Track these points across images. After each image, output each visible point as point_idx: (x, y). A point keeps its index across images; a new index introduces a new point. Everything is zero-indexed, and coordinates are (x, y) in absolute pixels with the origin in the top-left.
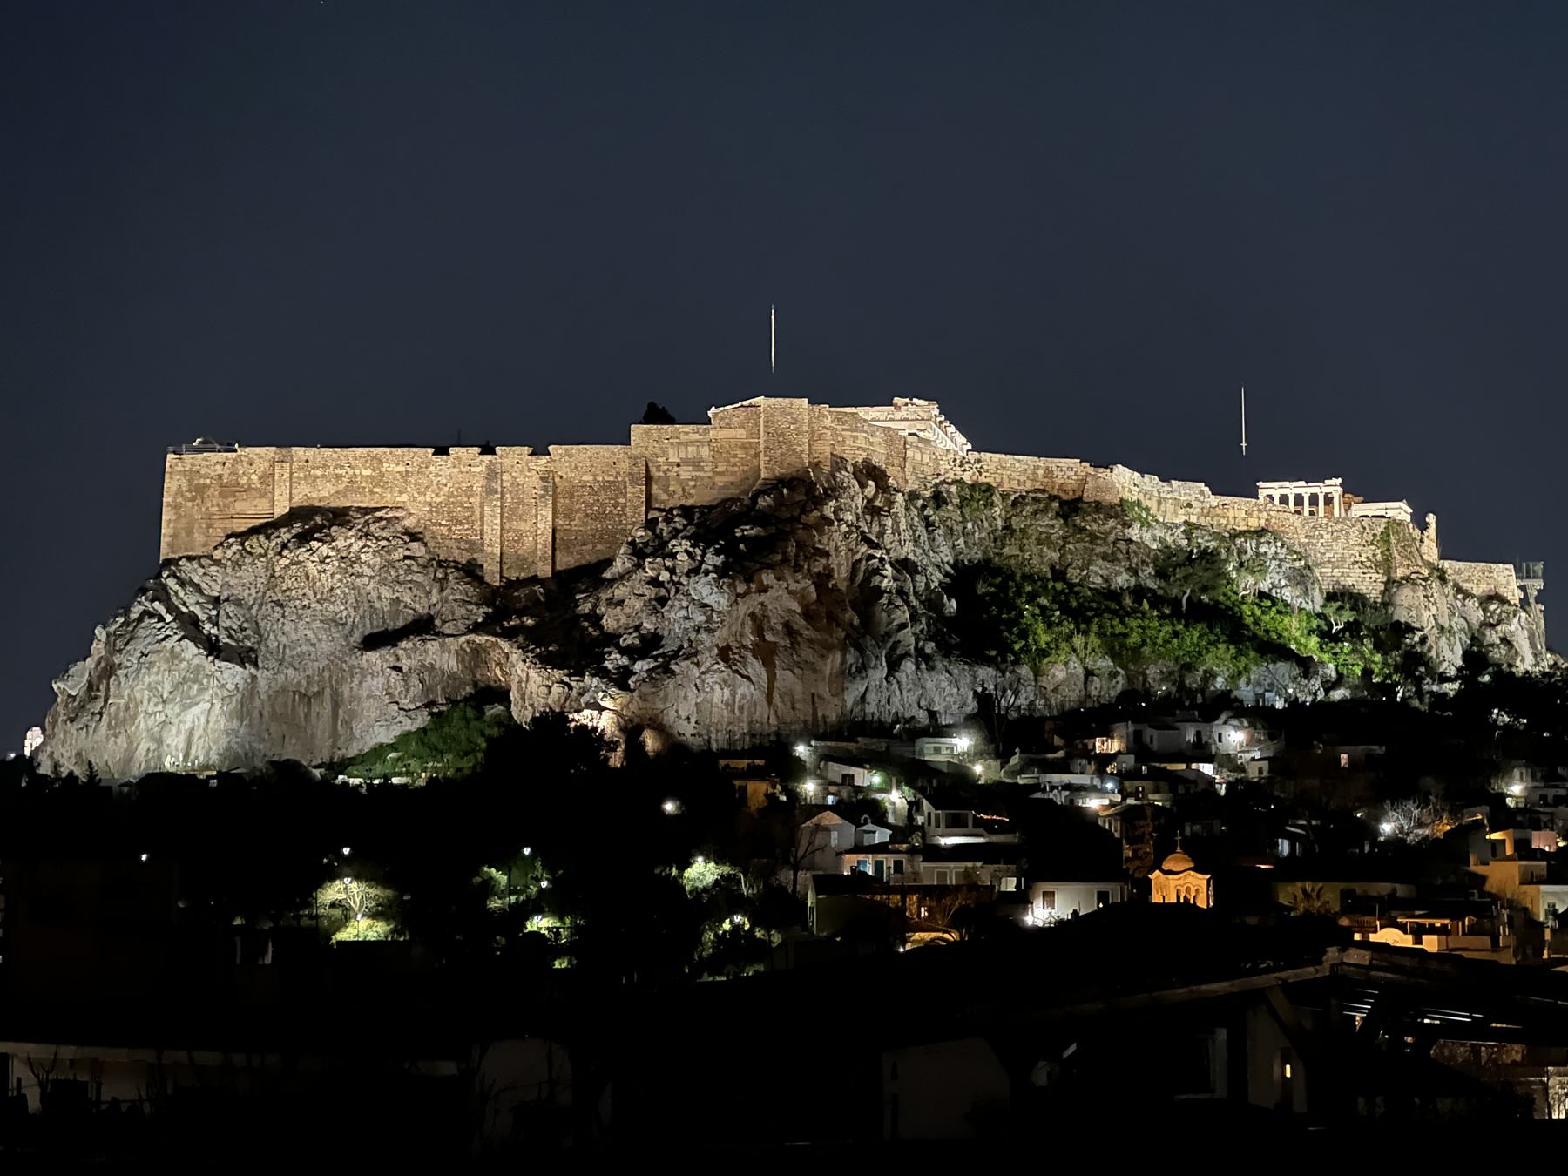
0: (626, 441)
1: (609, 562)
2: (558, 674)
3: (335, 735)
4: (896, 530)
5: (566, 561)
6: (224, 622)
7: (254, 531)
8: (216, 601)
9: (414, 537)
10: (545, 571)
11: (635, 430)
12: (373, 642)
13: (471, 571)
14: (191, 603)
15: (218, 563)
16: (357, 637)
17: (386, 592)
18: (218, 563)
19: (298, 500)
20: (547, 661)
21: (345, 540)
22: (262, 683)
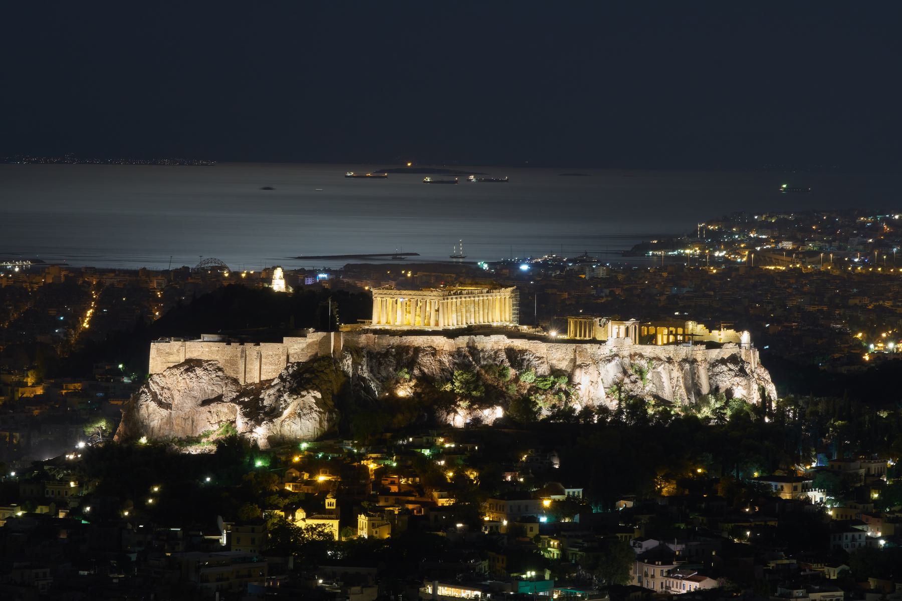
0: (282, 342)
1: (273, 380)
2: (246, 420)
3: (193, 430)
4: (362, 369)
5: (263, 378)
6: (164, 395)
7: (175, 367)
8: (163, 388)
9: (220, 369)
10: (257, 381)
11: (285, 339)
12: (206, 402)
13: (235, 381)
15: (164, 376)
16: (200, 402)
17: (210, 387)
18: (164, 376)
19: (188, 357)
20: (245, 415)
21: (199, 371)
22: (173, 415)
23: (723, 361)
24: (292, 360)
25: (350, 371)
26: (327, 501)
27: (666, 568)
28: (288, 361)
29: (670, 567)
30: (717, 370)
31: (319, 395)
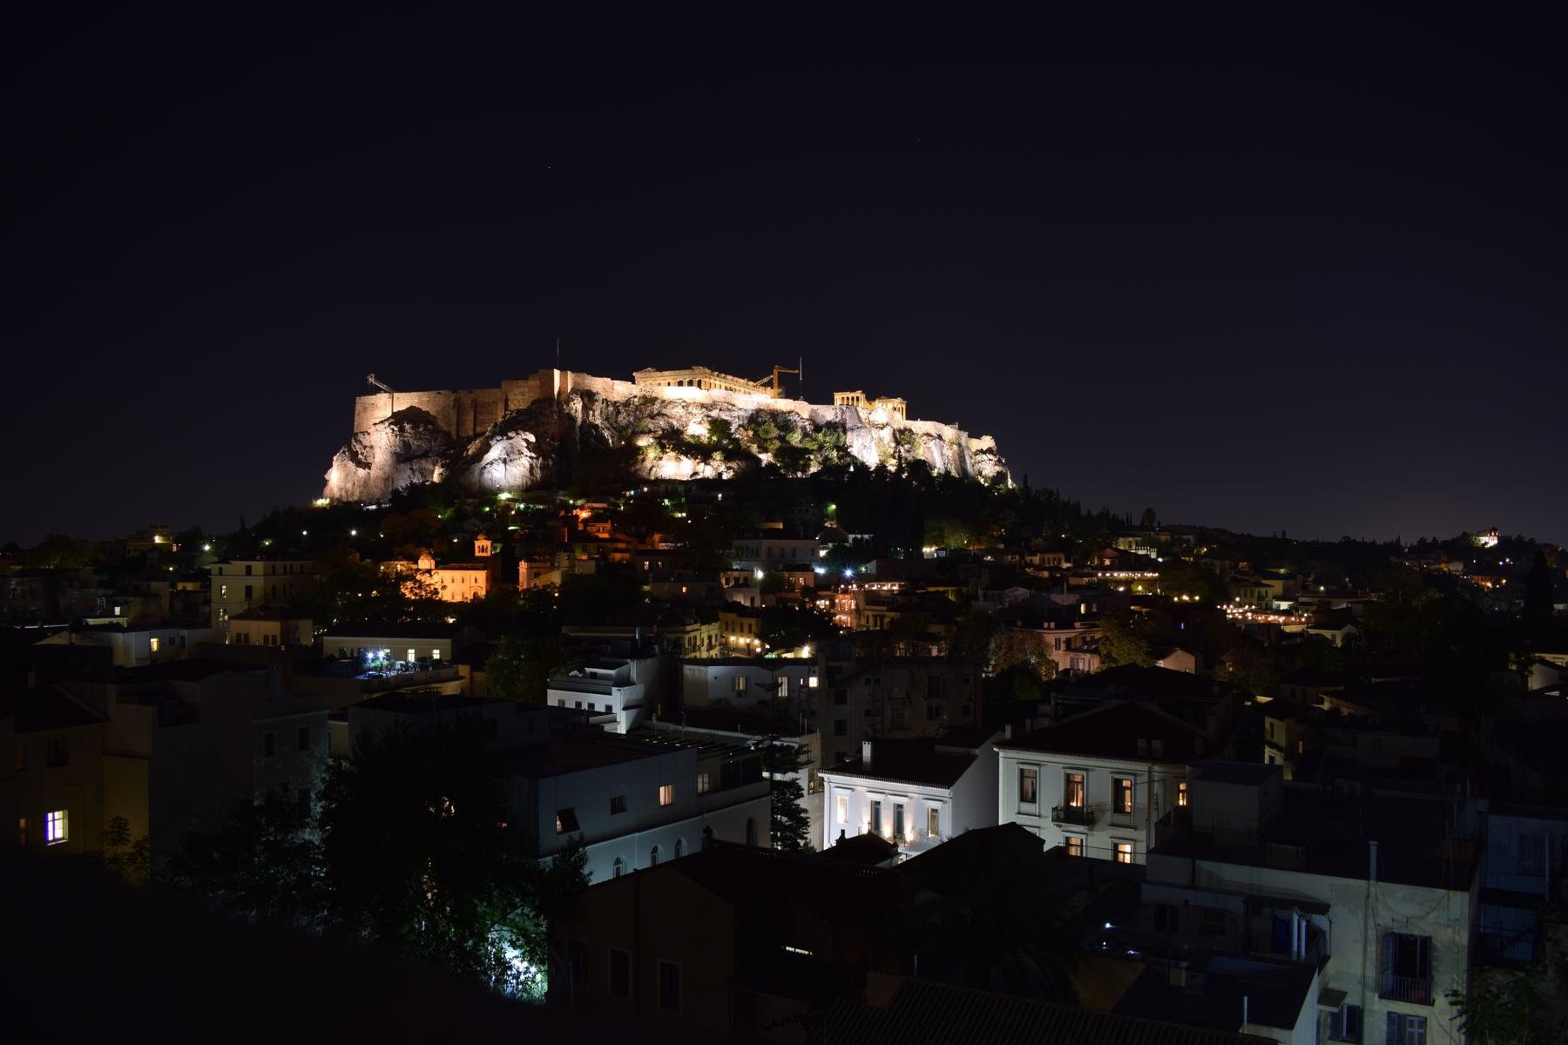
13: (448, 434)
14: (358, 448)
23: (982, 452)
24: (512, 407)
25: (579, 416)
26: (477, 544)
27: (1064, 635)
28: (506, 409)
29: (1070, 634)
30: (979, 458)
31: (532, 438)
